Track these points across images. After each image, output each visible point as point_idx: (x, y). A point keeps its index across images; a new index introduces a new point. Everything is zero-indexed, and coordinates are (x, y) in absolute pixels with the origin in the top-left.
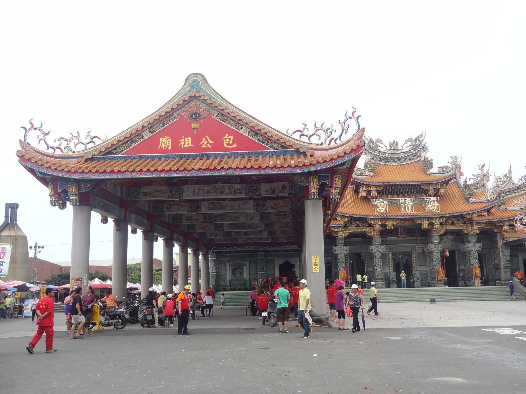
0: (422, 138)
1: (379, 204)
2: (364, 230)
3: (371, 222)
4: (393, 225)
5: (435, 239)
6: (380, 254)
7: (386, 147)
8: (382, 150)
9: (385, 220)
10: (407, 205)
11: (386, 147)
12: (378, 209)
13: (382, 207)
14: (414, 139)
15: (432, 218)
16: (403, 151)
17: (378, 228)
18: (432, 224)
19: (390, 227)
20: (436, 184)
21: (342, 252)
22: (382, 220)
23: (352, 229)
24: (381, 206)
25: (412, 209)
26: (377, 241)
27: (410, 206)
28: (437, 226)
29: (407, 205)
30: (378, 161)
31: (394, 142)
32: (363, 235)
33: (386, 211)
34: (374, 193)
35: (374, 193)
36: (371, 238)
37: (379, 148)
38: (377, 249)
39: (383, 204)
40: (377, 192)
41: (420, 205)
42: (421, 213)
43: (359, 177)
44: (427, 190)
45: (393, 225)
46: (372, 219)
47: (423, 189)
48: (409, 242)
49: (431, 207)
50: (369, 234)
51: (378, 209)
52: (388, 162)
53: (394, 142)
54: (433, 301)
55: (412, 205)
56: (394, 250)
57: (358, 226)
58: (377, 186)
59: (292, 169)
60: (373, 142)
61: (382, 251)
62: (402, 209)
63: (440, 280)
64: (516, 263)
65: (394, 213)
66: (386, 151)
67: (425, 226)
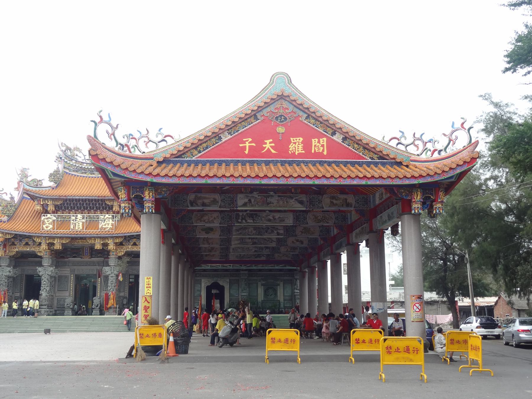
1: (46, 220)
2: (33, 249)
3: (38, 240)
4: (63, 244)
5: (112, 261)
6: (47, 277)
7: (84, 156)
8: (80, 160)
9: (54, 238)
10: (78, 223)
11: (84, 156)
12: (44, 226)
13: (49, 224)
15: (107, 238)
17: (44, 246)
18: (105, 245)
19: (58, 246)
20: (45, 199)
21: (4, 274)
22: (50, 238)
23: (20, 248)
24: (48, 223)
25: (83, 228)
26: (46, 262)
27: (81, 224)
28: (111, 247)
29: (78, 223)
30: (74, 171)
32: (34, 255)
33: (53, 229)
34: (51, 208)
35: (51, 208)
36: (41, 257)
37: (76, 157)
38: (46, 272)
39: (51, 220)
40: (56, 206)
41: (92, 223)
42: (92, 232)
43: (34, 189)
44: (111, 208)
45: (63, 244)
46: (38, 237)
47: (108, 205)
48: (93, 264)
49: (105, 225)
50: (39, 254)
51: (44, 226)
52: (85, 173)
54: (47, 331)
55: (83, 223)
56: (76, 273)
57: (27, 244)
58: (53, 199)
59: (176, 179)
60: (70, 149)
61: (50, 273)
62: (72, 227)
63: (110, 308)
64: (198, 290)
65: (62, 231)
66: (84, 161)
67: (98, 247)
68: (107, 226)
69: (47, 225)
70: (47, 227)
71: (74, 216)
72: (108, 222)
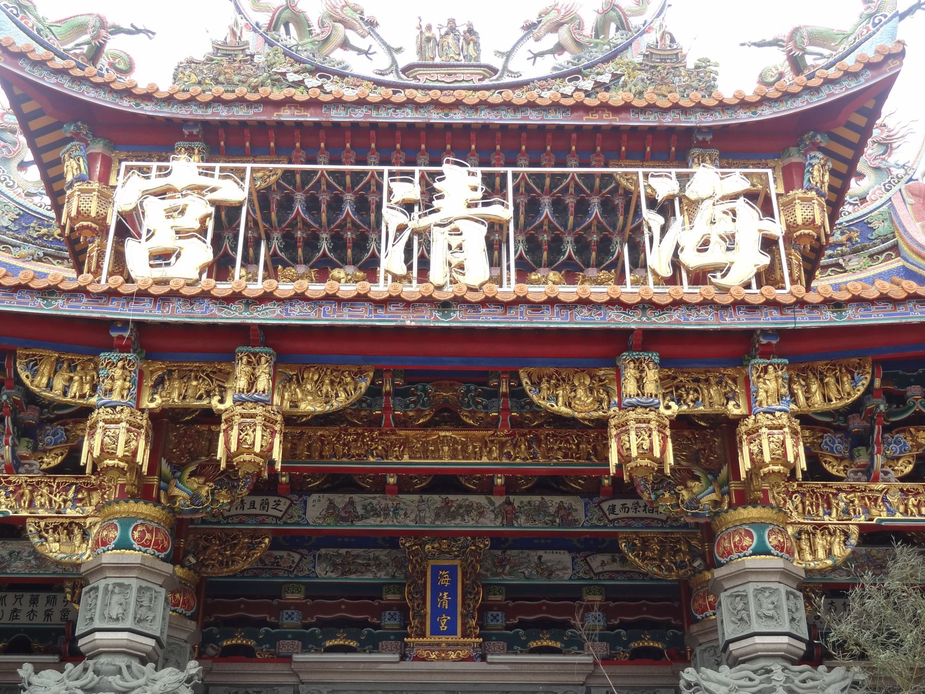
0: (648, 16)
14: (590, 21)
16: (507, 80)
17: (116, 436)
18: (708, 441)
28: (772, 442)
31: (452, 29)
33: (220, 267)
36: (66, 584)
37: (338, 55)
49: (704, 246)
53: (452, 29)
55: (495, 228)
62: (392, 259)
68: (716, 255)
69: (165, 240)
70: (162, 257)
71: (407, 177)
72: (726, 225)
